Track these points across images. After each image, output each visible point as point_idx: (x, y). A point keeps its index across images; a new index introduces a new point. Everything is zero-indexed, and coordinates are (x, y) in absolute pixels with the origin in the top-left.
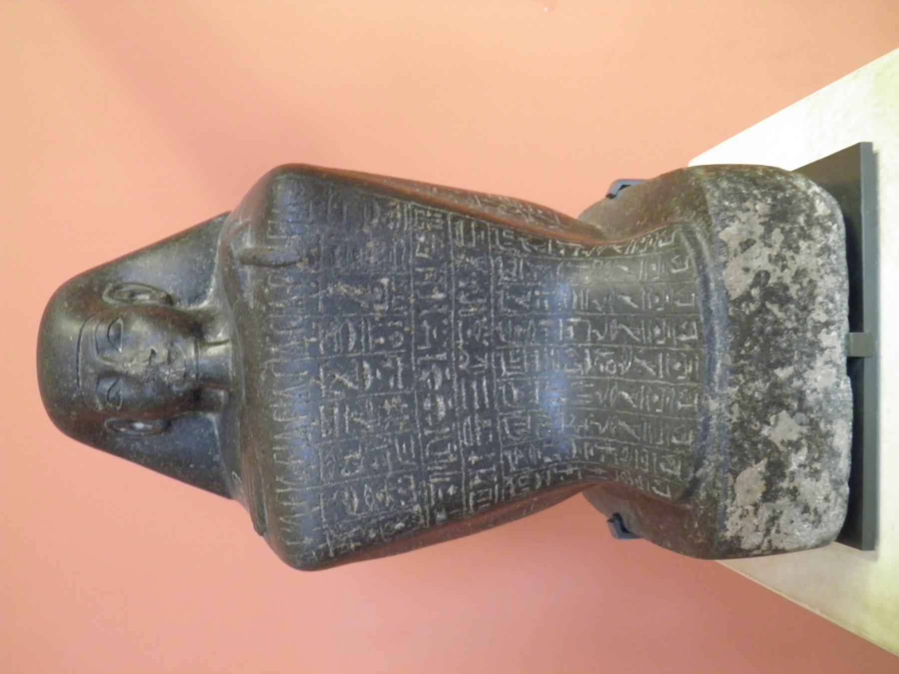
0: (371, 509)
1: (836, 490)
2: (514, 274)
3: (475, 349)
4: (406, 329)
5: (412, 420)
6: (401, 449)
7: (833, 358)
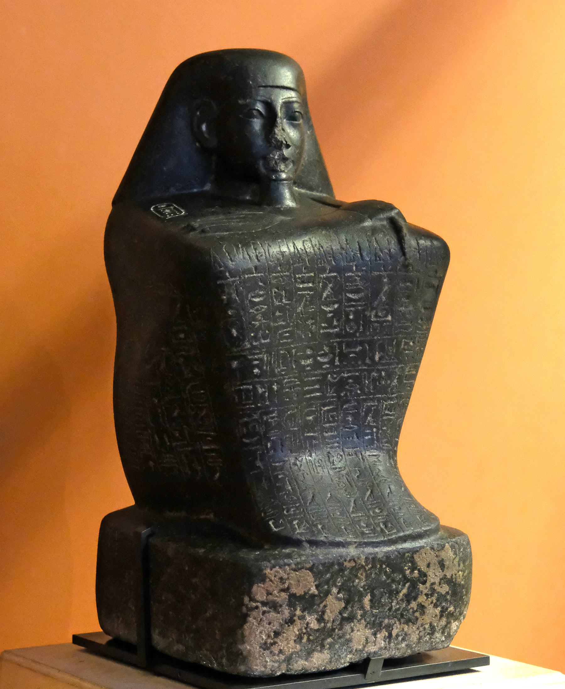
0: (251, 311)
1: (284, 661)
2: (387, 412)
3: (341, 385)
4: (358, 334)
5: (302, 340)
6: (286, 332)
7: (369, 644)
